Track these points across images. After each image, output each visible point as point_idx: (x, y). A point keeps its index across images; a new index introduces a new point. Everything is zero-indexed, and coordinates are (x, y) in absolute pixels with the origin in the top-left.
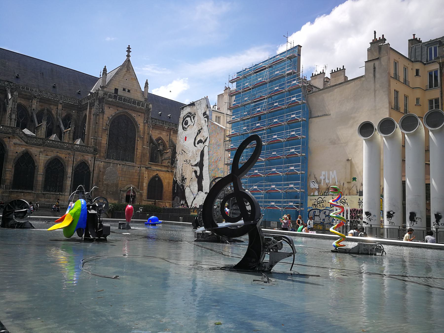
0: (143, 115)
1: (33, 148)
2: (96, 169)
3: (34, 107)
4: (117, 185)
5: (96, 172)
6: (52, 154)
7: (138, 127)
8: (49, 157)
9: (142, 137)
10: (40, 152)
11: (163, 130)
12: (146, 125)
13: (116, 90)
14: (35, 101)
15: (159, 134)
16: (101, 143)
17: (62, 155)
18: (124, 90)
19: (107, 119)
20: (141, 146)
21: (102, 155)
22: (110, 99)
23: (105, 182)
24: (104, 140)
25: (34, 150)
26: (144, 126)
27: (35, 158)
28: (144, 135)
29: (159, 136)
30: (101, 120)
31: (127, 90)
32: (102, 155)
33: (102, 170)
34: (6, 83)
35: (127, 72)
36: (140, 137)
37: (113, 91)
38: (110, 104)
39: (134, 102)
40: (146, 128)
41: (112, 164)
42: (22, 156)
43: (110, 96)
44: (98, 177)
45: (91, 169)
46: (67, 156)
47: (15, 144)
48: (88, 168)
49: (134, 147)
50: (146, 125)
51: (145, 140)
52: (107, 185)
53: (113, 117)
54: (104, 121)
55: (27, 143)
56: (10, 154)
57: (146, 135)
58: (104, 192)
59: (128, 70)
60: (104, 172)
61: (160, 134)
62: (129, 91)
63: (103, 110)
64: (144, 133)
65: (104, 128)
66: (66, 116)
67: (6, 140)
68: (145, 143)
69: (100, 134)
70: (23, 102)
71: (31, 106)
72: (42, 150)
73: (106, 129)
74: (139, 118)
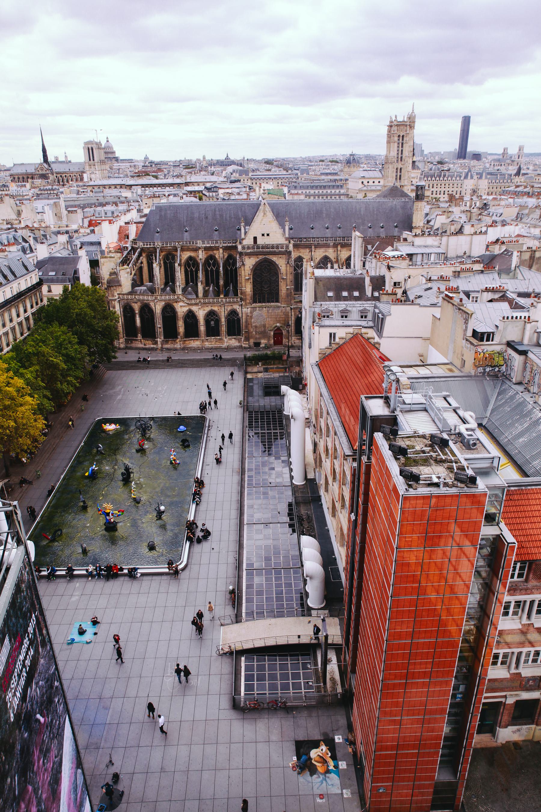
0: (284, 256)
1: (194, 307)
2: (244, 315)
3: (200, 257)
4: (264, 326)
5: (243, 318)
6: (208, 309)
7: (280, 270)
8: (206, 311)
9: (285, 277)
10: (199, 309)
11: (329, 247)
12: (288, 265)
13: (255, 239)
14: (200, 252)
15: (323, 252)
16: (245, 292)
17: (216, 309)
18: (263, 235)
19: (249, 269)
20: (284, 287)
21: (248, 301)
22: (249, 251)
23: (253, 325)
24: (248, 288)
25: (194, 308)
26: (287, 267)
27: (197, 314)
28: (287, 276)
29: (324, 254)
30: (243, 272)
31: (266, 235)
32: (248, 301)
33: (249, 314)
34: (177, 243)
35: (264, 216)
36: (283, 279)
37: (252, 242)
38: (250, 255)
39: (273, 247)
40: (288, 268)
41: (257, 309)
42: (188, 314)
43: (248, 248)
44: (246, 322)
45: (240, 315)
46: (220, 308)
47: (181, 306)
48: (238, 315)
49: (279, 288)
50: (288, 265)
51: (288, 280)
52: (256, 327)
53: (254, 266)
54: (246, 271)
55: (188, 304)
56: (179, 314)
57: (288, 275)
58: (254, 333)
59: (264, 214)
60: (251, 317)
61: (326, 252)
62: (268, 235)
63: (243, 262)
64: (287, 274)
65: (247, 278)
66: (228, 257)
67: (175, 305)
68: (288, 283)
69: (243, 284)
70: (192, 254)
71: (198, 256)
72: (200, 307)
73: (249, 279)
74: (281, 260)
